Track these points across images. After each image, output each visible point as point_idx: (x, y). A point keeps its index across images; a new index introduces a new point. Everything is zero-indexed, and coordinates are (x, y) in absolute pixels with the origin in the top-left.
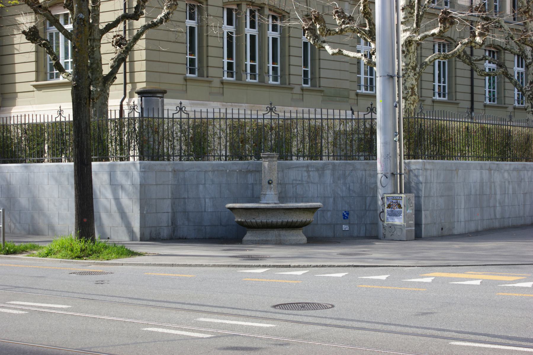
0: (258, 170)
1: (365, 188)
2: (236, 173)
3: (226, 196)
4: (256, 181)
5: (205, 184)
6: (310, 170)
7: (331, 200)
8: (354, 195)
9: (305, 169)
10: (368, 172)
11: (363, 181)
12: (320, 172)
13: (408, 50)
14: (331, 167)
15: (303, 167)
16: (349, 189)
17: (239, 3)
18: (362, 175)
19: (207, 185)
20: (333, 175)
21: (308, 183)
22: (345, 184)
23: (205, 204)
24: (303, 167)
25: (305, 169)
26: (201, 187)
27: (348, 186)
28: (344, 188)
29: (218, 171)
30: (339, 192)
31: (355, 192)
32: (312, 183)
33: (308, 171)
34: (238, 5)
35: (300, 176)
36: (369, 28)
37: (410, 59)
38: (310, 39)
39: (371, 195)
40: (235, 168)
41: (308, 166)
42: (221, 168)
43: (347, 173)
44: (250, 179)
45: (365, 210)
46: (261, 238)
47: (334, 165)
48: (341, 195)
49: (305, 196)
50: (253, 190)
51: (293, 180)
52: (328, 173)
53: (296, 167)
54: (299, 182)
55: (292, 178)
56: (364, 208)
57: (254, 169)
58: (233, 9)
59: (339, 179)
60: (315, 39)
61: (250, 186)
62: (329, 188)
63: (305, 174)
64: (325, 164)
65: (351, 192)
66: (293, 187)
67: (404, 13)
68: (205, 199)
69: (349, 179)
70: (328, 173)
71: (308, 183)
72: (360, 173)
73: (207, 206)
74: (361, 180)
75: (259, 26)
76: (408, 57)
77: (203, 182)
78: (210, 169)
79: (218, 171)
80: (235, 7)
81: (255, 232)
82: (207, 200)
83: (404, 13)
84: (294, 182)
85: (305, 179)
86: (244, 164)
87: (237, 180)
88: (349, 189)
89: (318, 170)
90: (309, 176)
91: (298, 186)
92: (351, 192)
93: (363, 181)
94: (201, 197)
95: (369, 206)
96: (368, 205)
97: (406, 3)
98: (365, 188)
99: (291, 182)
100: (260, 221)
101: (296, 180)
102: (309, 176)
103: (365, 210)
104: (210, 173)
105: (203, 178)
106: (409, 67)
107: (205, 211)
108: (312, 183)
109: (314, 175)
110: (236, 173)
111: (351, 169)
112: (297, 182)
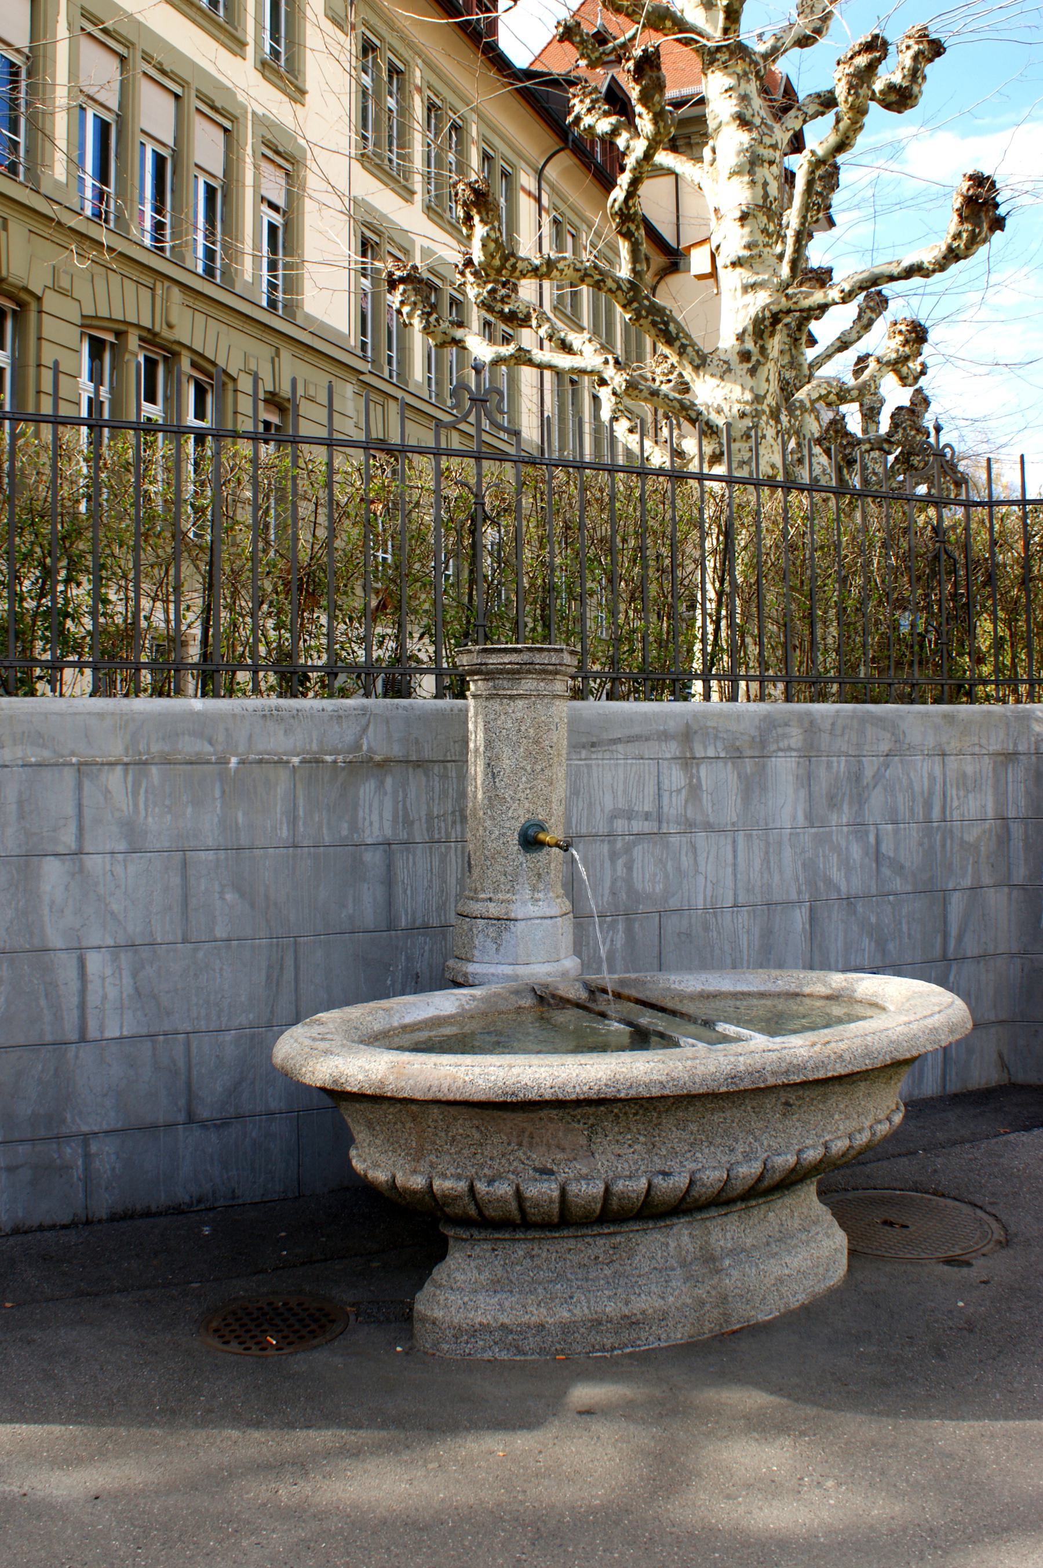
0: (437, 760)
1: (944, 846)
2: (284, 774)
3: (220, 932)
4: (408, 823)
5: (80, 852)
6: (699, 753)
7: (799, 917)
8: (898, 884)
9: (672, 749)
10: (952, 762)
11: (936, 814)
12: (749, 766)
13: (763, 350)
14: (795, 737)
15: (665, 736)
16: (878, 857)
17: (123, 327)
18: (932, 778)
19: (95, 863)
20: (807, 780)
21: (689, 826)
22: (859, 827)
23: (83, 992)
24: (665, 736)
25: (672, 749)
26: (53, 874)
27: (872, 839)
28: (856, 852)
29: (166, 761)
30: (836, 875)
31: (899, 869)
32: (709, 828)
33: (688, 762)
34: (118, 334)
35: (651, 789)
36: (633, 270)
37: (768, 380)
38: (410, 315)
39: (968, 882)
40: (275, 741)
42: (190, 746)
43: (869, 772)
44: (376, 813)
45: (945, 958)
46: (582, 1310)
47: (811, 727)
48: (844, 888)
49: (673, 903)
50: (389, 881)
51: (613, 817)
52: (784, 767)
53: (631, 739)
54: (647, 827)
55: (609, 805)
56: (937, 952)
57: (396, 751)
58: (102, 342)
59: (833, 802)
60: (429, 314)
61: (373, 859)
62: (788, 853)
63: (676, 777)
64: (769, 723)
65: (886, 871)
66: (613, 856)
67: (747, 230)
68: (80, 953)
69: (877, 799)
70: (784, 767)
71: (689, 826)
72: (923, 770)
73: (93, 999)
74: (928, 805)
75: (166, 399)
76: (763, 372)
77: (68, 839)
78: (116, 749)
79: (166, 761)
80: (110, 338)
81: (520, 1250)
82: (95, 962)
83: (747, 230)
84: (620, 826)
85: (674, 805)
86: (338, 717)
87: (293, 822)
88: (878, 857)
89: (735, 755)
90: (694, 790)
91: (637, 852)
92: (886, 871)
93: (936, 814)
94: (56, 940)
95: (960, 938)
96: (954, 931)
97: (754, 198)
98: (944, 846)
99: (602, 828)
100: (597, 1189)
101: (629, 815)
102: (694, 790)
103: (945, 958)
104: (114, 779)
105: (70, 810)
106: (765, 407)
107: (83, 1039)
108: (709, 828)
109: (719, 779)
110: (284, 774)
111: (885, 747)
112: (637, 826)
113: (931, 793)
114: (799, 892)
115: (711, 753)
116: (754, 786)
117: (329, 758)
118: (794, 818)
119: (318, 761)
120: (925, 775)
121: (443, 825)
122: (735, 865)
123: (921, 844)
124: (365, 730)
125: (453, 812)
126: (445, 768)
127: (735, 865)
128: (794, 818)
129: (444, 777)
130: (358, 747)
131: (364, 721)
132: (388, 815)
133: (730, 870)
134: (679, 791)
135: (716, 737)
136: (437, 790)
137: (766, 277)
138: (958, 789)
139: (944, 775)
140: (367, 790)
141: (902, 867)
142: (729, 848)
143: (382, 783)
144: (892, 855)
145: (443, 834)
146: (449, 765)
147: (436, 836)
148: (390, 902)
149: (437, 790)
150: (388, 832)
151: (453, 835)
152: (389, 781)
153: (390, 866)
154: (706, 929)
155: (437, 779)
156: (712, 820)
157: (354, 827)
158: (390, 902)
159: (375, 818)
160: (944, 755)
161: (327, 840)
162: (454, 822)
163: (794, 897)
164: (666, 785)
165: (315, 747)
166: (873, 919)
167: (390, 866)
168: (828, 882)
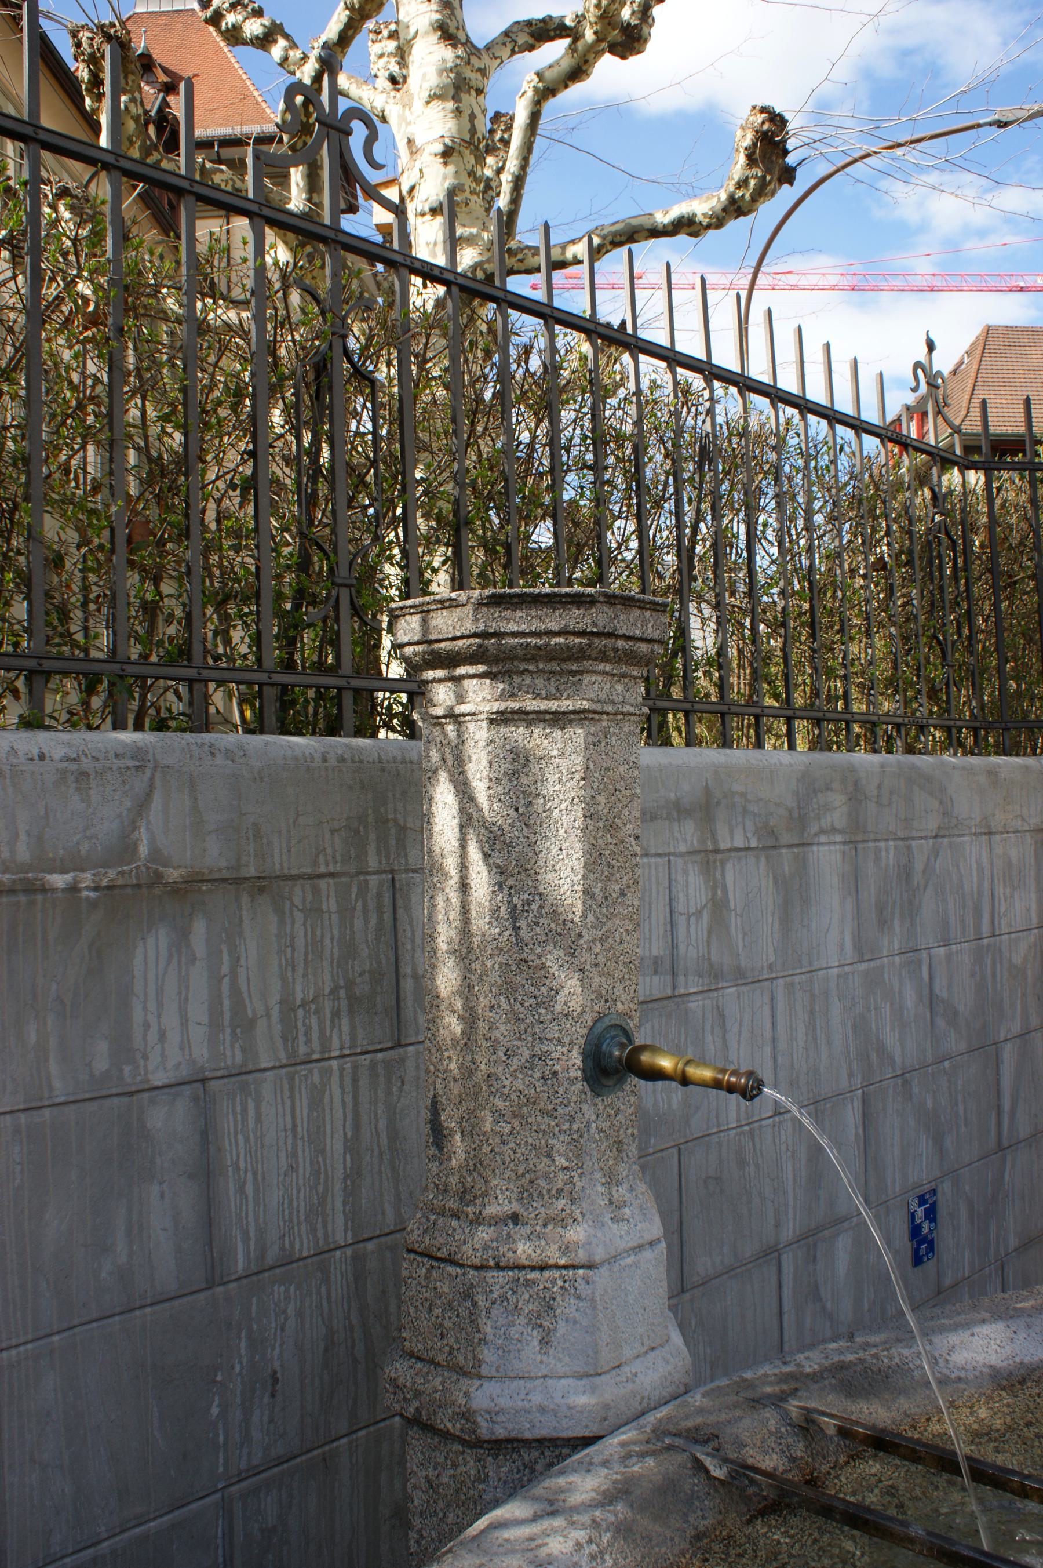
21: (715, 975)
25: (687, 835)
30: (890, 1038)
32: (741, 977)
33: (710, 858)
39: (1016, 1028)
41: (705, 807)
50: (206, 1171)
57: (215, 856)
61: (168, 1121)
62: (836, 1009)
63: (693, 889)
67: (451, 169)
71: (715, 975)
74: (978, 912)
83: (451, 169)
85: (693, 939)
86: (79, 775)
88: (932, 1001)
89: (770, 844)
90: (719, 906)
92: (941, 1023)
97: (459, 131)
108: (741, 977)
111: (932, 824)
113: (980, 894)
114: (851, 1075)
115: (739, 843)
116: (794, 896)
117: (59, 880)
118: (842, 947)
119: (34, 889)
120: (974, 866)
121: (314, 1021)
122: (774, 1040)
123: (973, 975)
124: (142, 805)
125: (334, 991)
126: (316, 891)
127: (774, 1040)
128: (842, 947)
129: (314, 911)
130: (127, 849)
131: (139, 784)
132: (199, 1012)
133: (768, 1049)
134: (699, 913)
135: (745, 811)
136: (300, 942)
137: (474, 231)
138: (1005, 886)
139: (992, 864)
140: (150, 953)
141: (956, 1013)
142: (767, 1011)
143: (183, 934)
144: (945, 995)
145: (316, 1044)
146: (323, 884)
147: (302, 1049)
148: (209, 1218)
149: (300, 942)
150: (201, 1052)
151: (336, 1043)
152: (199, 928)
153: (206, 1135)
154: (742, 1163)
155: (299, 916)
156: (743, 964)
157: (123, 1048)
158: (209, 1218)
159: (171, 1020)
160: (990, 833)
161: (60, 1089)
162: (336, 1014)
163: (844, 1084)
164: (681, 908)
165: (23, 853)
166: (930, 1104)
167: (206, 1135)
168: (881, 1049)
